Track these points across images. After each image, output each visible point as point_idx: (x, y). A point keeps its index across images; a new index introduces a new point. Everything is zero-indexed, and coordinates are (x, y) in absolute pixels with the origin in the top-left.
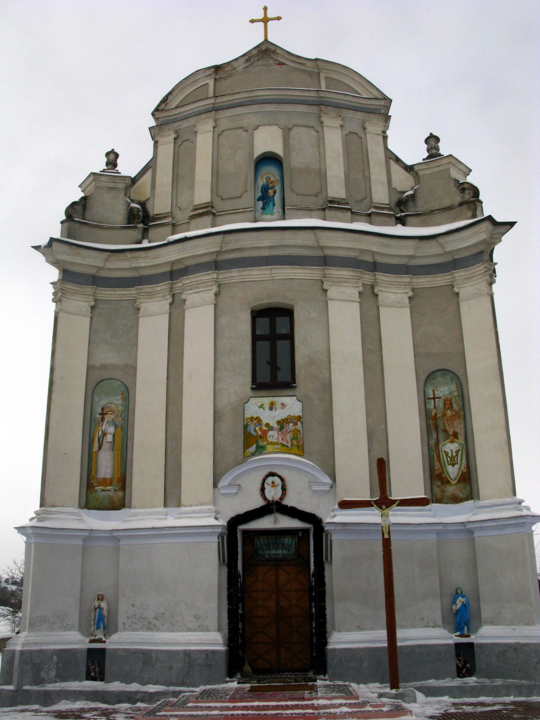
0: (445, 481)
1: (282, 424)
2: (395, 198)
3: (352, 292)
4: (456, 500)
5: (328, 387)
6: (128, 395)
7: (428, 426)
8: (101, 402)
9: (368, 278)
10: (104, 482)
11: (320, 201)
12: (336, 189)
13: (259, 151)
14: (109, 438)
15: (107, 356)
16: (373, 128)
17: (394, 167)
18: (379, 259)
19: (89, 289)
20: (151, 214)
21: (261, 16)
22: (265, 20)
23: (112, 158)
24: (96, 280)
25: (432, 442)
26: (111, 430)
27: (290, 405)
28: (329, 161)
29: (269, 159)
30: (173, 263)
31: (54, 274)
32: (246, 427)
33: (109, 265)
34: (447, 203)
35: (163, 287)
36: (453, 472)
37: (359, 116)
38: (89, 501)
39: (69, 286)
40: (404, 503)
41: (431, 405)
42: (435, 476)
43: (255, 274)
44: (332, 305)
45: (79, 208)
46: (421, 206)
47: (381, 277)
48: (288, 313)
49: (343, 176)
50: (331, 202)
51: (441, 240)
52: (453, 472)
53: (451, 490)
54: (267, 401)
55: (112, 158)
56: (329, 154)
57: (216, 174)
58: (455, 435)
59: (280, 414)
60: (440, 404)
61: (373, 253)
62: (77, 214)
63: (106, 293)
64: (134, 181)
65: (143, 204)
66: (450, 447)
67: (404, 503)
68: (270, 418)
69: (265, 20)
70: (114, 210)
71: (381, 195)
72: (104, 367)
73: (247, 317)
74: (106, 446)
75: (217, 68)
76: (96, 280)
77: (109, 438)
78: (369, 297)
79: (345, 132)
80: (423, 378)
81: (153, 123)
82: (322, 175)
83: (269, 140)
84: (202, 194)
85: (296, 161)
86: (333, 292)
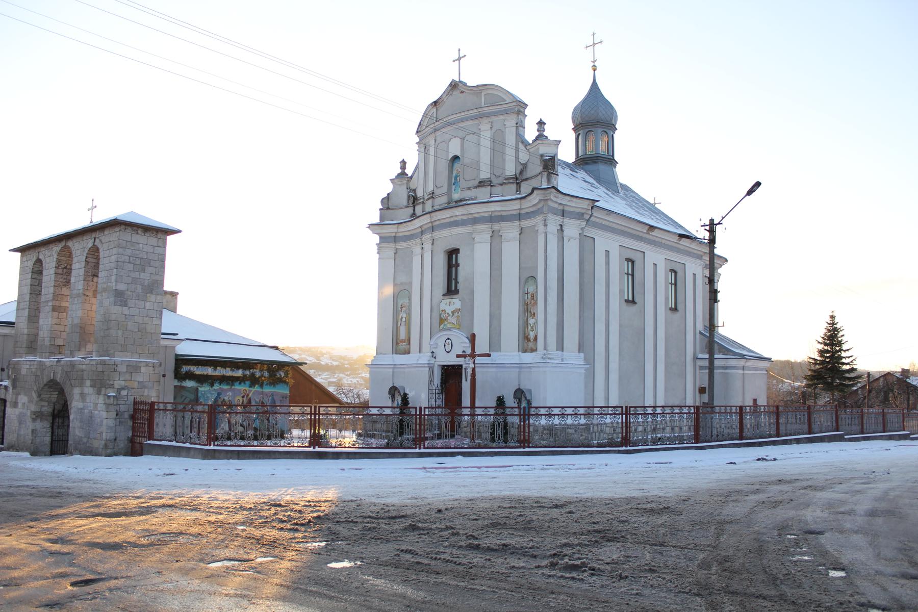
0: (529, 340)
1: (453, 312)
2: (520, 168)
3: (487, 236)
5: (472, 292)
8: (400, 302)
9: (496, 227)
10: (402, 341)
11: (476, 183)
12: (485, 175)
13: (451, 156)
14: (404, 320)
16: (511, 121)
17: (521, 146)
18: (504, 213)
19: (393, 245)
21: (457, 57)
22: (459, 59)
23: (403, 163)
24: (395, 239)
26: (404, 315)
27: (456, 303)
29: (456, 158)
30: (421, 227)
31: (376, 239)
33: (400, 230)
35: (418, 240)
37: (502, 117)
38: (396, 351)
39: (383, 245)
40: (480, 355)
43: (445, 233)
44: (477, 246)
45: (386, 201)
46: (529, 173)
47: (503, 224)
49: (489, 163)
50: (480, 182)
52: (532, 335)
53: (531, 345)
54: (448, 301)
55: (403, 163)
59: (453, 308)
62: (387, 203)
63: (400, 245)
64: (411, 177)
66: (531, 321)
67: (480, 355)
68: (449, 310)
69: (459, 59)
70: (402, 198)
71: (511, 169)
72: (402, 284)
75: (435, 103)
76: (395, 239)
78: (496, 237)
79: (493, 131)
80: (523, 281)
81: (417, 140)
83: (454, 149)
84: (430, 188)
85: (465, 160)
86: (478, 238)
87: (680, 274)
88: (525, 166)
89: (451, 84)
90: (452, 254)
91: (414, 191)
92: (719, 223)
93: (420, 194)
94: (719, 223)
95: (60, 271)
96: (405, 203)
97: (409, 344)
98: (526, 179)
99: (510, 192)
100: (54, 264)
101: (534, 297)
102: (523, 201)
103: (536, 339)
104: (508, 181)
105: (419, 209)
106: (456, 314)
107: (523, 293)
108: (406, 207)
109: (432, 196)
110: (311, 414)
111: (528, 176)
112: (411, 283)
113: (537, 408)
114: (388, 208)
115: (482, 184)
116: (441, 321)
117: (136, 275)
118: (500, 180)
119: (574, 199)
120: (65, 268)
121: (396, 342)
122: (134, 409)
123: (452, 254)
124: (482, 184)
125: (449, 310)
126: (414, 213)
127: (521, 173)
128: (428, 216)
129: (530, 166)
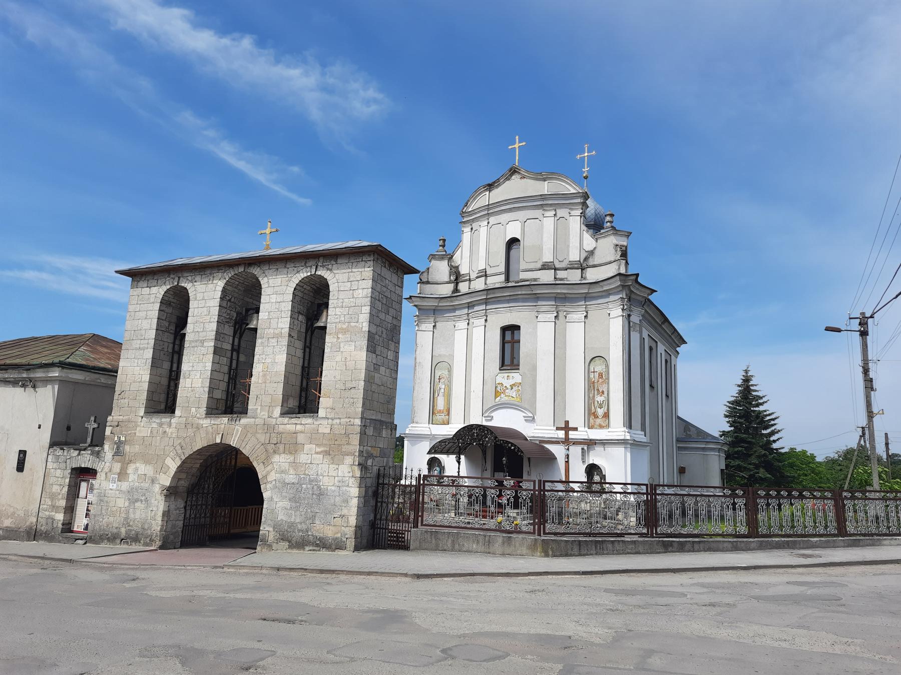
0: (596, 417)
2: (584, 255)
4: (601, 427)
5: (534, 368)
6: (450, 371)
7: (589, 387)
11: (539, 266)
12: (548, 257)
14: (442, 390)
15: (440, 351)
20: (462, 273)
25: (591, 395)
26: (443, 386)
27: (516, 377)
28: (545, 239)
32: (496, 387)
34: (608, 260)
36: (600, 412)
38: (431, 421)
41: (592, 376)
42: (590, 414)
46: (596, 260)
48: (518, 328)
51: (601, 284)
52: (600, 412)
53: (598, 421)
56: (545, 235)
57: (488, 252)
58: (603, 392)
59: (512, 382)
60: (597, 375)
61: (565, 294)
65: (457, 267)
66: (600, 399)
68: (507, 383)
71: (575, 256)
72: (440, 355)
73: (498, 333)
74: (441, 394)
77: (442, 390)
82: (540, 249)
83: (514, 231)
84: (482, 266)
85: (526, 243)
87: (669, 363)
88: (592, 253)
89: (511, 169)
90: (510, 333)
91: (457, 267)
92: (872, 317)
93: (463, 270)
94: (872, 317)
95: (224, 304)
96: (447, 279)
97: (448, 415)
98: (594, 266)
99: (574, 276)
100: (218, 294)
101: (604, 377)
102: (592, 286)
103: (607, 415)
104: (572, 266)
105: (463, 287)
106: (515, 388)
107: (588, 372)
108: (447, 283)
109: (484, 274)
110: (647, 494)
111: (595, 263)
112: (452, 356)
113: (610, 484)
114: (428, 283)
115: (545, 267)
116: (497, 394)
117: (382, 316)
118: (563, 265)
119: (640, 288)
120: (230, 300)
121: (433, 411)
122: (378, 484)
123: (510, 333)
124: (545, 267)
125: (507, 383)
126: (456, 290)
127: (586, 259)
128: (485, 292)
129: (597, 252)
